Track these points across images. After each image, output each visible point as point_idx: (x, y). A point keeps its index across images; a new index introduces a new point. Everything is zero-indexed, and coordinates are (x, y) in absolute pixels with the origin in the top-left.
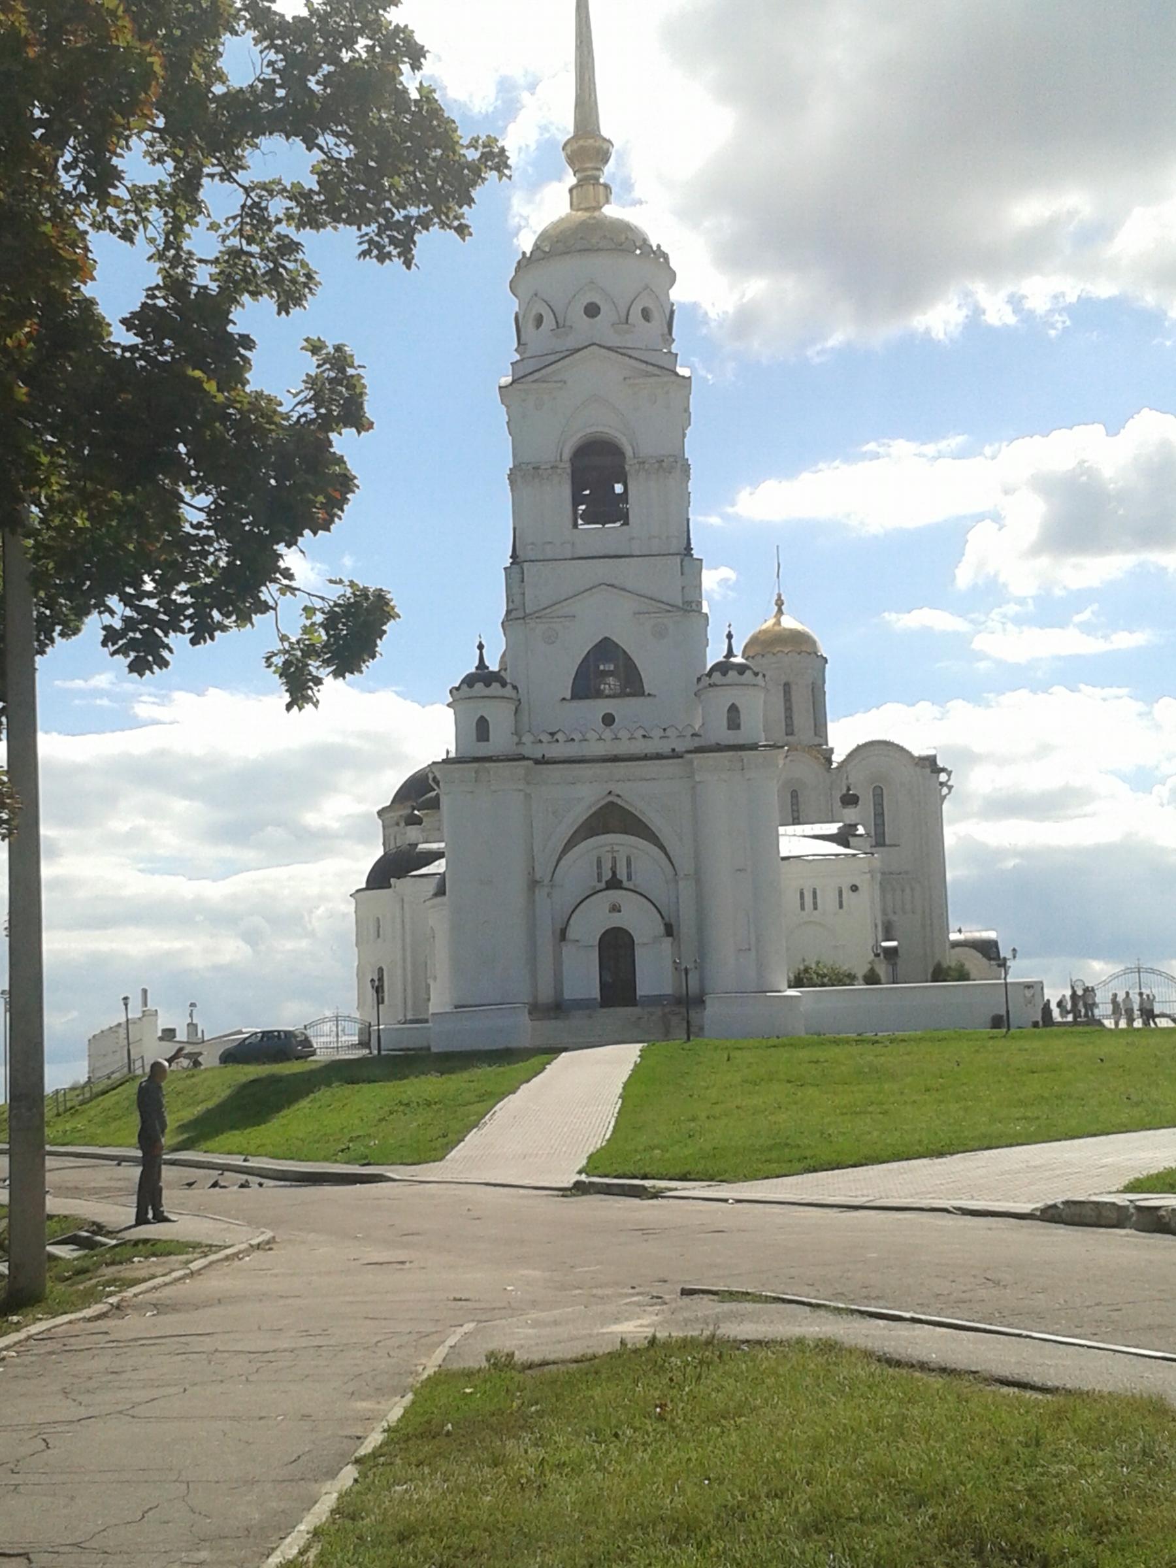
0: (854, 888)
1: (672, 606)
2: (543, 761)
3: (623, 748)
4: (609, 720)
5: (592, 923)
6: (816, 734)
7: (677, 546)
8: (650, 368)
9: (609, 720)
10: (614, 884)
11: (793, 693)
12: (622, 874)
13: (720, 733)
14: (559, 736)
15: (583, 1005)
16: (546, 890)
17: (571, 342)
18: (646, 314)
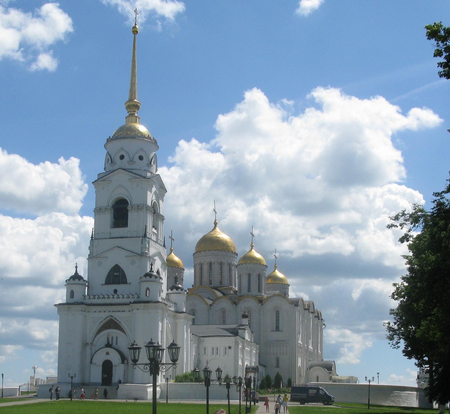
0: (230, 348)
1: (137, 254)
2: (88, 305)
3: (120, 301)
4: (115, 291)
5: (100, 358)
6: (259, 291)
7: (142, 234)
8: (137, 176)
9: (115, 291)
10: (109, 345)
11: (252, 277)
12: (110, 343)
13: (143, 297)
14: (97, 297)
15: (95, 384)
16: (89, 347)
17: (115, 167)
18: (141, 158)
